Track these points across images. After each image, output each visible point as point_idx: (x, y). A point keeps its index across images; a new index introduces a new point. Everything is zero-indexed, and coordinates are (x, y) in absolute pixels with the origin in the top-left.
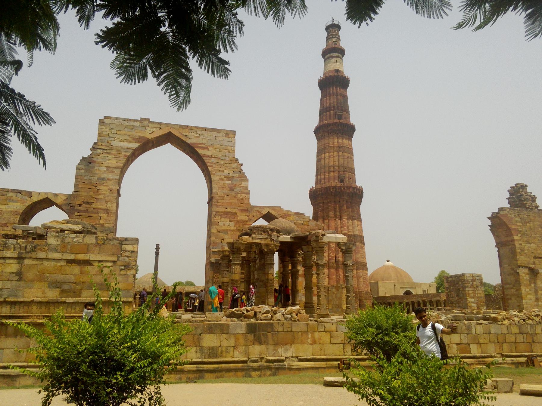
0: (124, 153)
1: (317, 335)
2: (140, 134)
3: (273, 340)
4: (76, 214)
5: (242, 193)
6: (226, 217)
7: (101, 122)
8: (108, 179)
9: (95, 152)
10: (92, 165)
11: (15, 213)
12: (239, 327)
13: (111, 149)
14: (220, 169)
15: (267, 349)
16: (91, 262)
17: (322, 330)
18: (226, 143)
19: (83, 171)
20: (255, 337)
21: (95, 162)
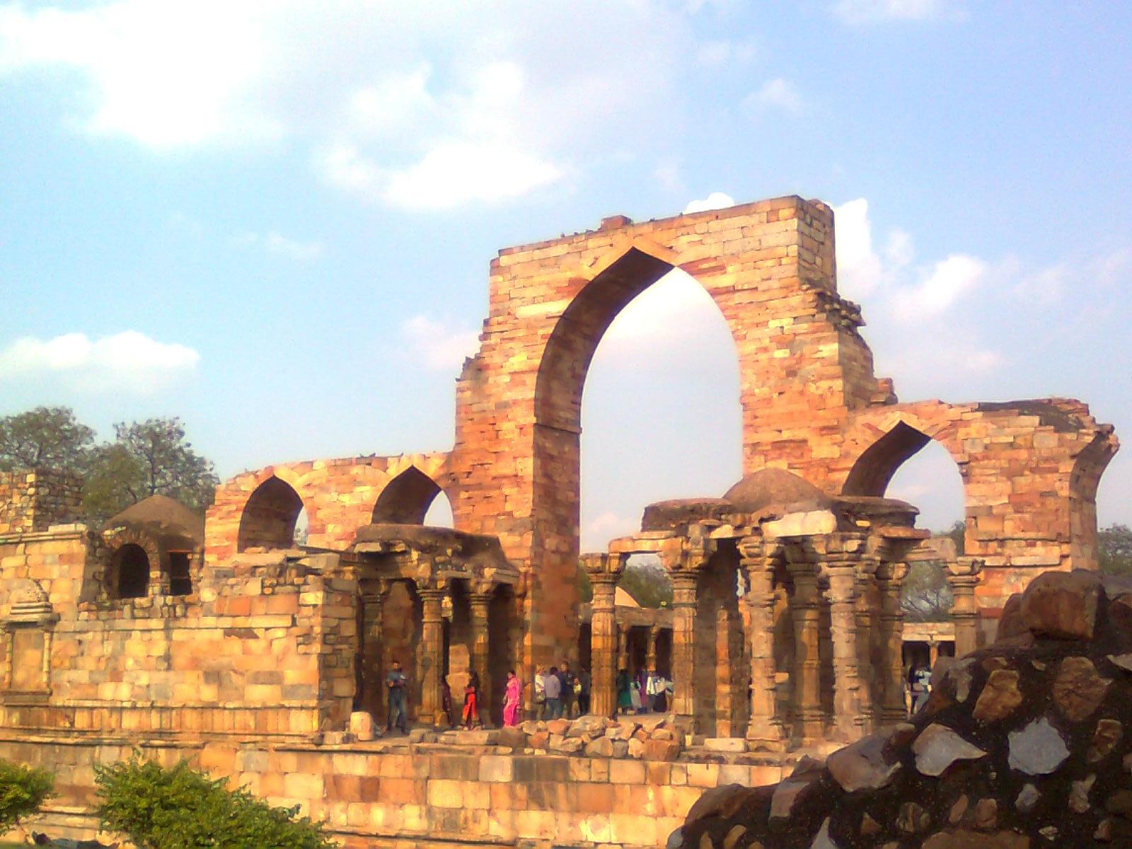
0: (541, 332)
1: (667, 791)
2: (569, 275)
3: (569, 801)
4: (463, 495)
5: (821, 378)
6: (780, 457)
7: (495, 267)
8: (515, 402)
9: (487, 342)
10: (484, 375)
11: (362, 508)
12: (500, 768)
13: (516, 328)
14: (757, 320)
15: (557, 820)
16: (255, 631)
17: (680, 783)
18: (770, 241)
19: (468, 394)
20: (529, 791)
21: (487, 367)
